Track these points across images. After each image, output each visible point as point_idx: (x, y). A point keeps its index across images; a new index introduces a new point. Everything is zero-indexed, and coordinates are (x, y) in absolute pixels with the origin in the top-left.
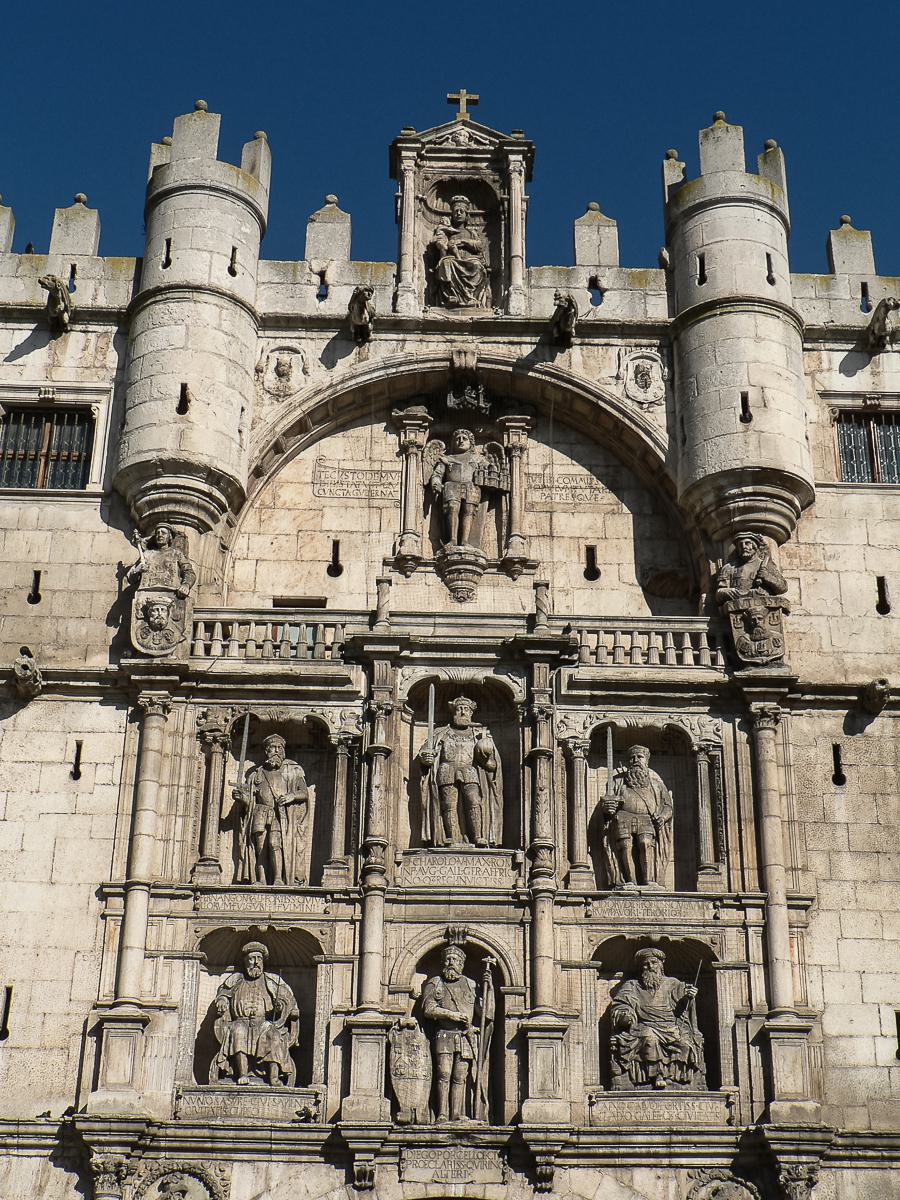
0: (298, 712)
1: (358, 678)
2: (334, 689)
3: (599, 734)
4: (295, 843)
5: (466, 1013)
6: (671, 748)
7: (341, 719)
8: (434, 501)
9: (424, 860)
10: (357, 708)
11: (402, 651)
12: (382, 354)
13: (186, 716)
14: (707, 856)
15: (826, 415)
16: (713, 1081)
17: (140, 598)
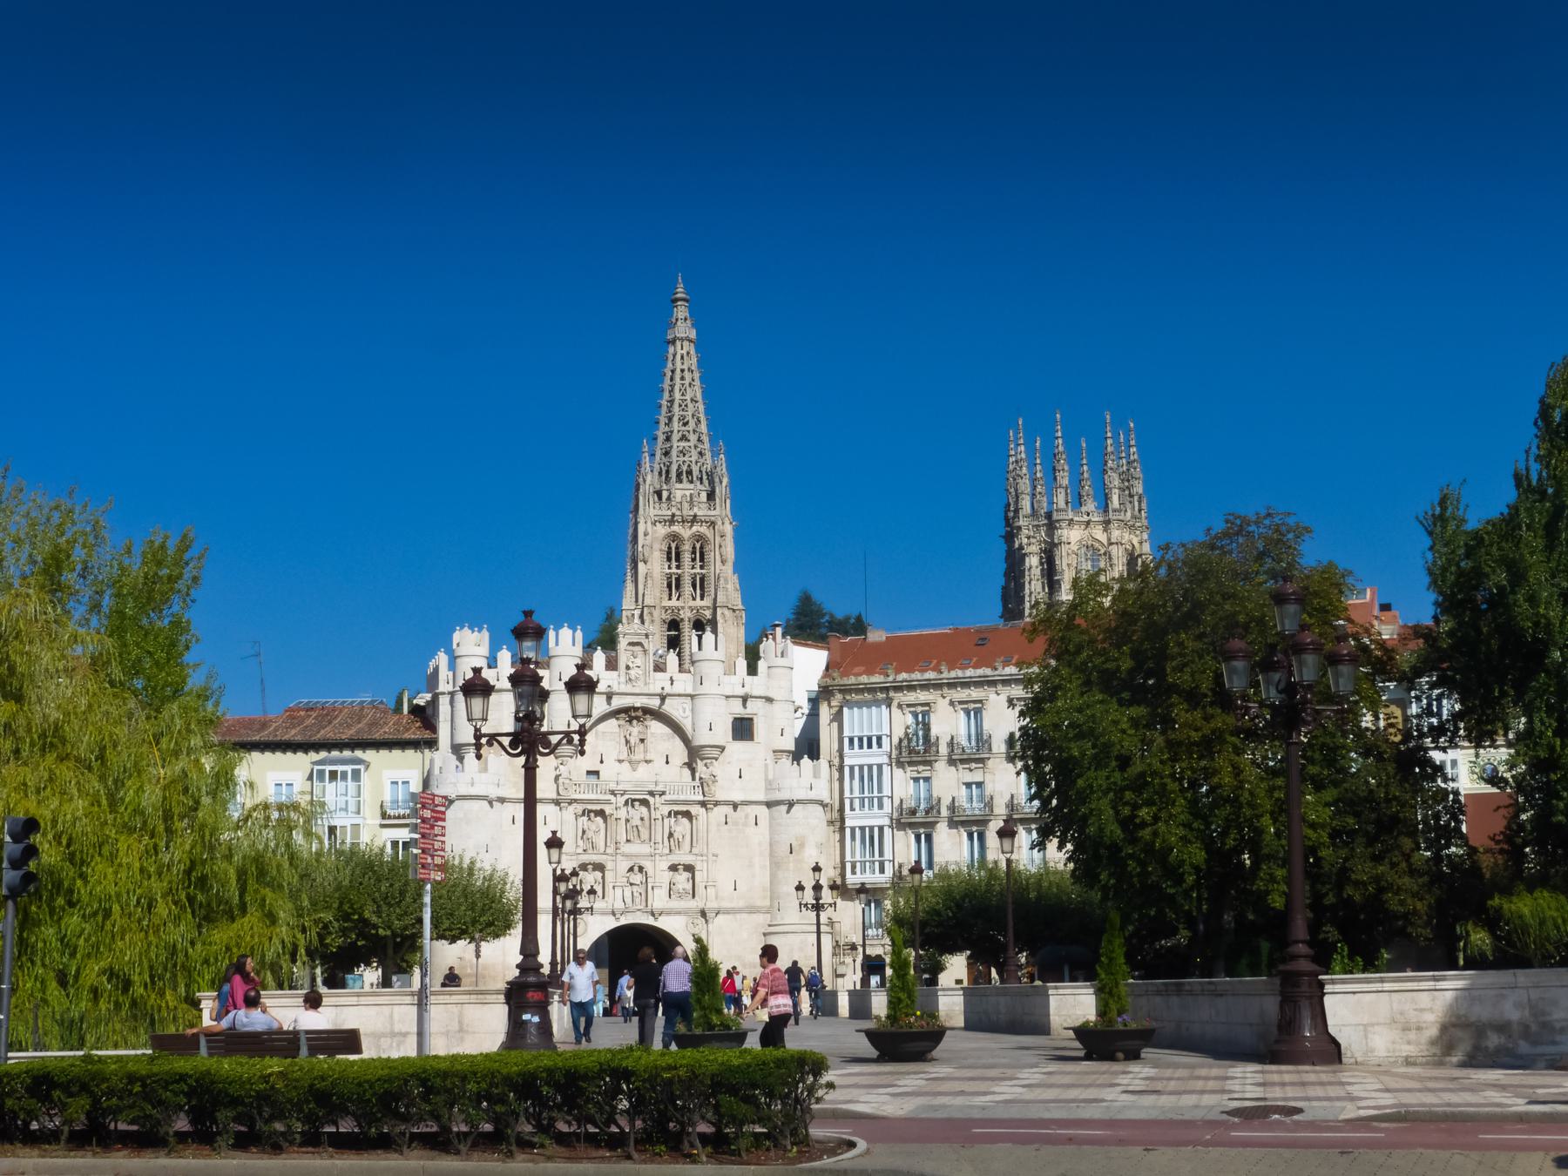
0: (598, 807)
1: (612, 798)
2: (608, 802)
3: (670, 813)
4: (600, 841)
5: (638, 883)
6: (687, 815)
7: (608, 810)
8: (627, 742)
9: (628, 844)
10: (613, 806)
11: (624, 793)
12: (618, 702)
13: (571, 808)
14: (694, 844)
15: (731, 720)
16: (694, 896)
17: (561, 780)
